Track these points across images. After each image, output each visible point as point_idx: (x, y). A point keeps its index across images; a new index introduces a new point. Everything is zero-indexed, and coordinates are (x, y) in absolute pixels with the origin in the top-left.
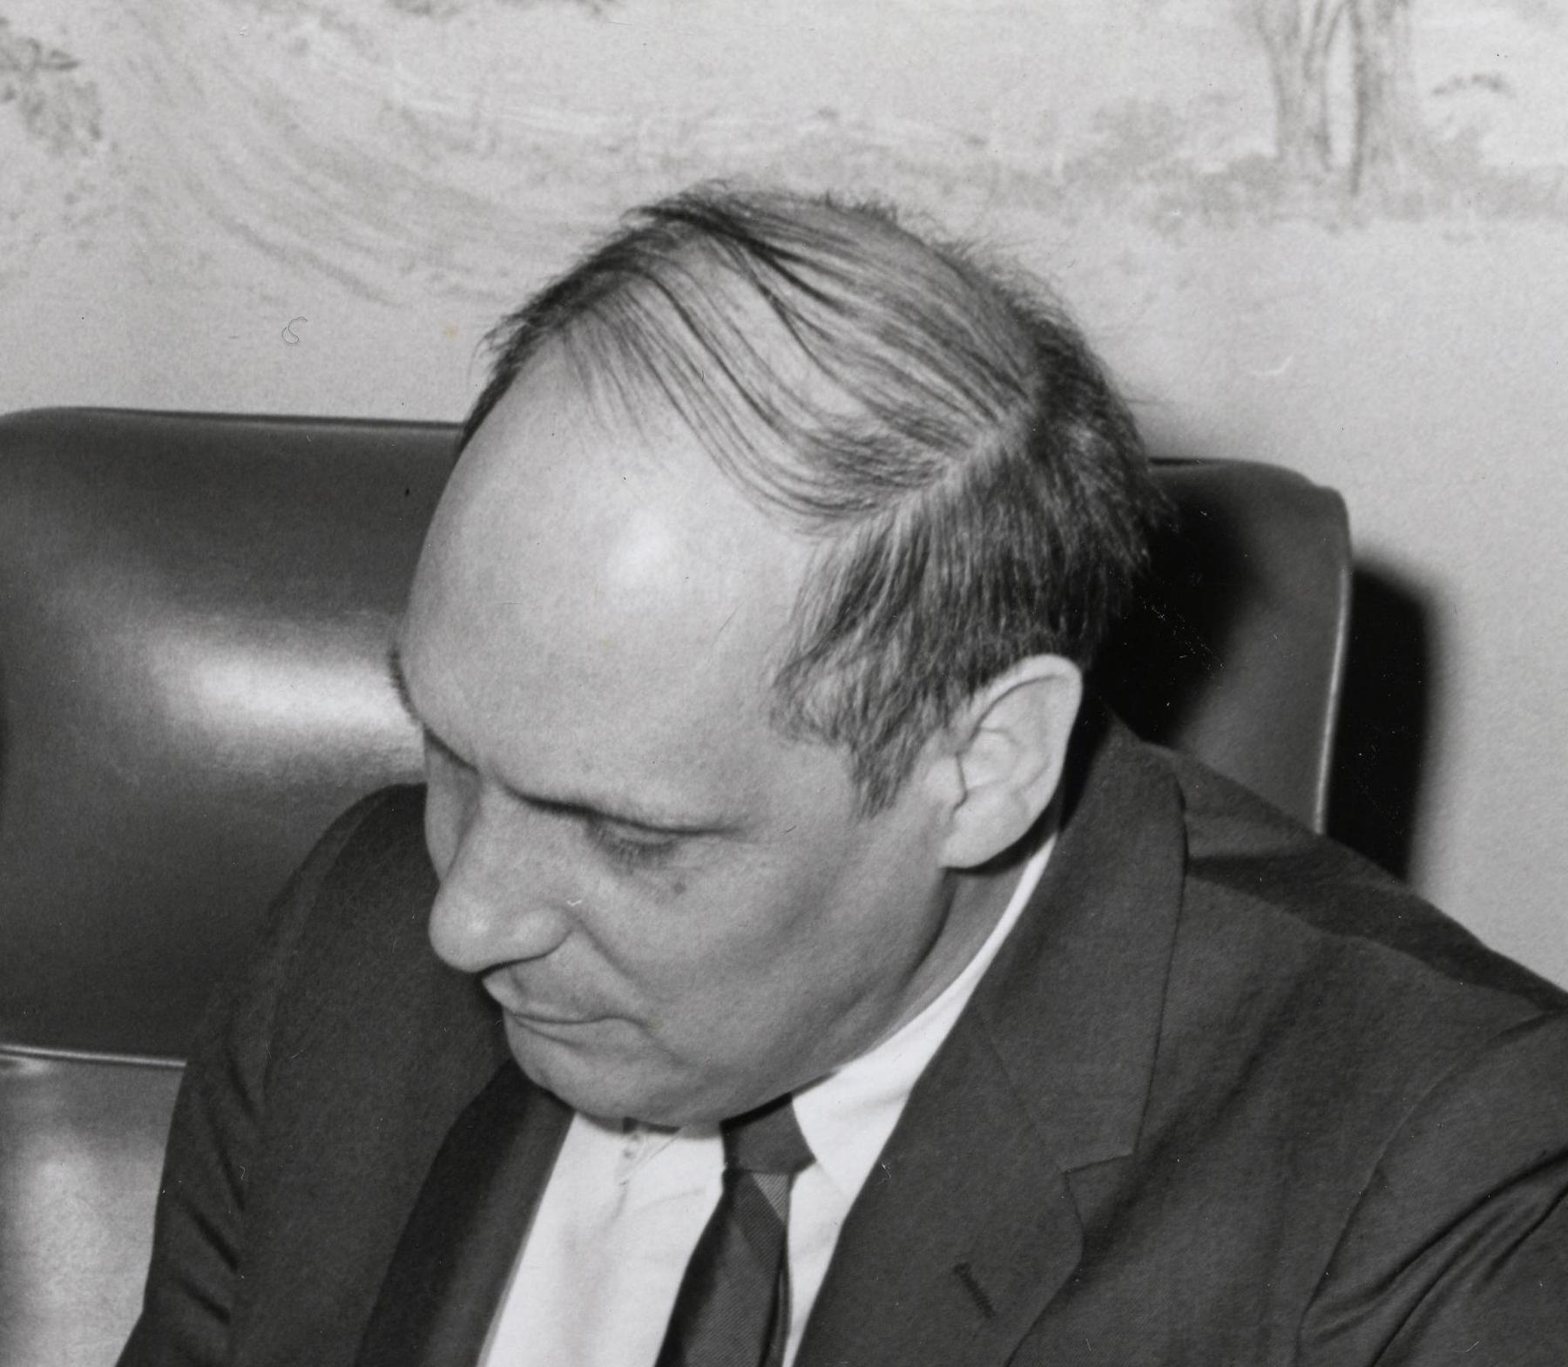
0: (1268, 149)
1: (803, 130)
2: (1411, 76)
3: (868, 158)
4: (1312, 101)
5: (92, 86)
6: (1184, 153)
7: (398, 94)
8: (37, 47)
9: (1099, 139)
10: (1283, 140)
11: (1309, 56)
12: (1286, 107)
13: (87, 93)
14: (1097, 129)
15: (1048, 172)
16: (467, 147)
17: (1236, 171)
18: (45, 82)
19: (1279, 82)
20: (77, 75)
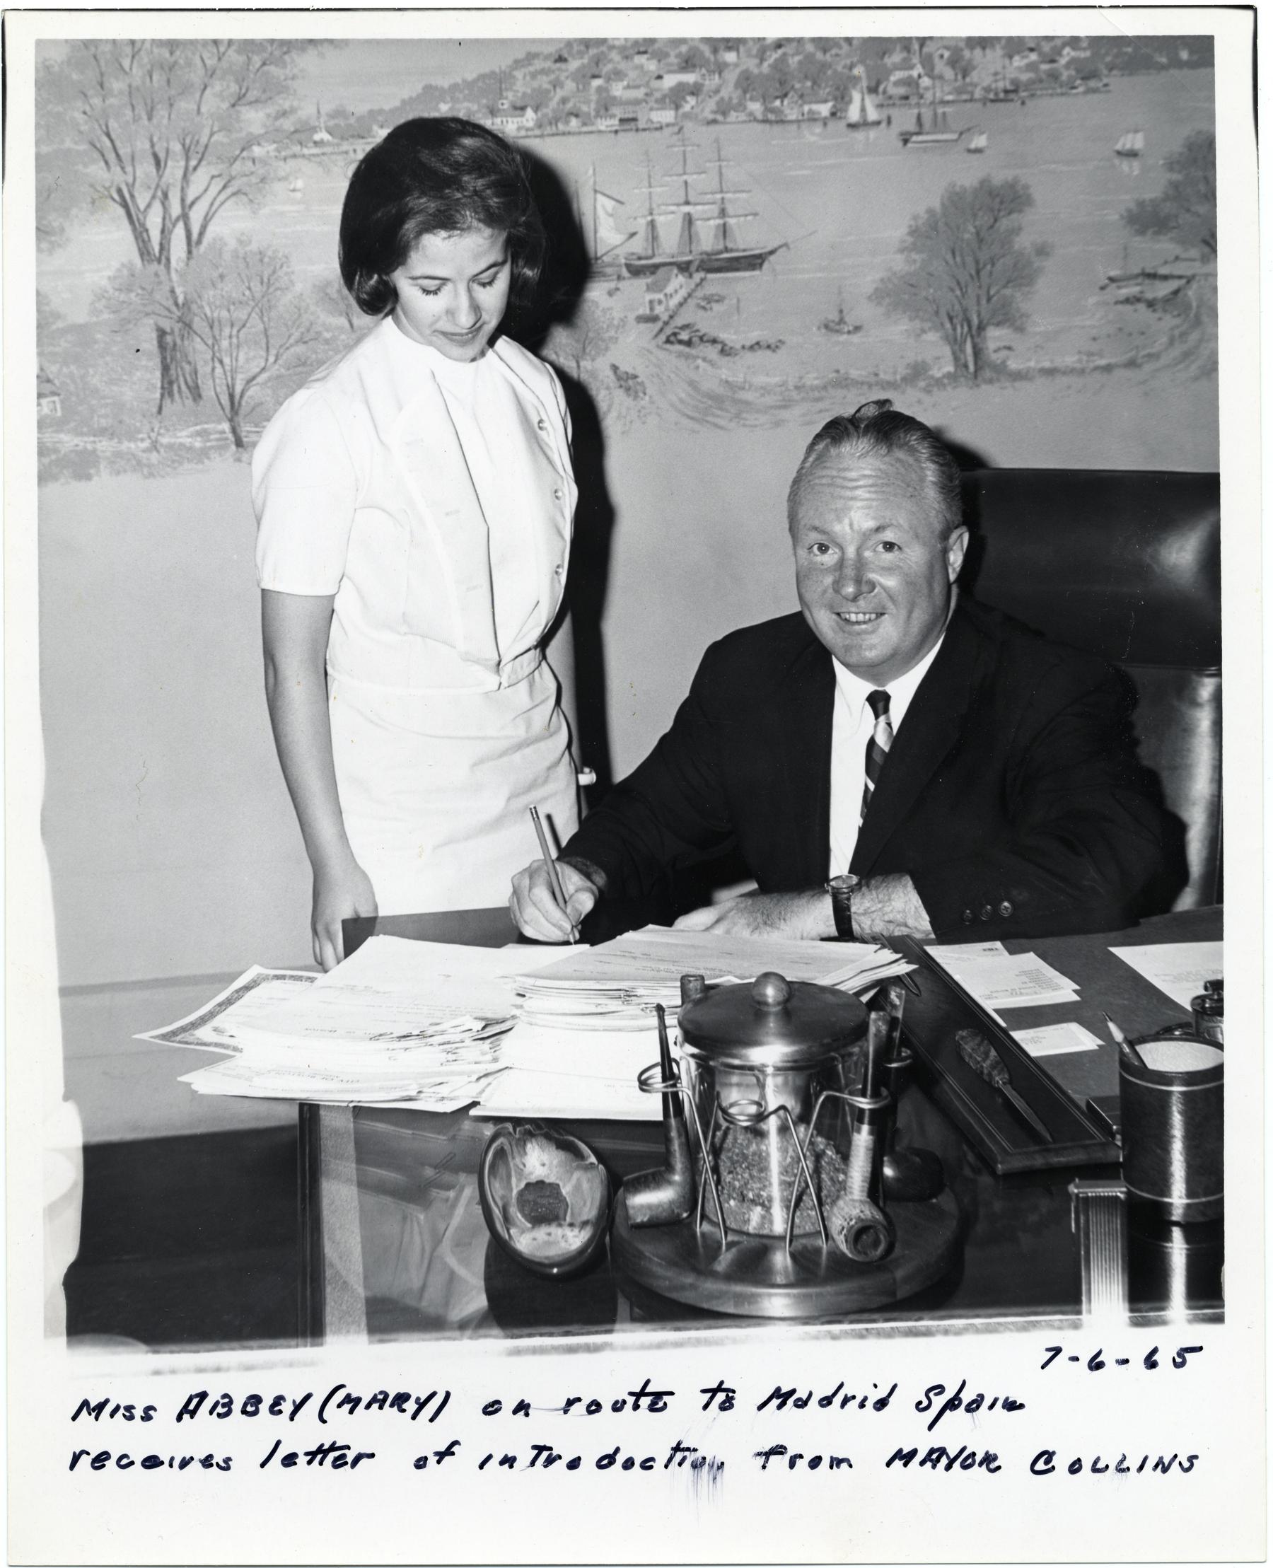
0: (950, 368)
2: (987, 348)
3: (849, 381)
4: (962, 356)
5: (643, 382)
6: (931, 373)
7: (724, 377)
8: (627, 373)
9: (909, 371)
10: (956, 366)
12: (956, 359)
13: (642, 384)
15: (896, 381)
16: (743, 388)
17: (944, 376)
18: (630, 382)
19: (954, 353)
20: (639, 380)
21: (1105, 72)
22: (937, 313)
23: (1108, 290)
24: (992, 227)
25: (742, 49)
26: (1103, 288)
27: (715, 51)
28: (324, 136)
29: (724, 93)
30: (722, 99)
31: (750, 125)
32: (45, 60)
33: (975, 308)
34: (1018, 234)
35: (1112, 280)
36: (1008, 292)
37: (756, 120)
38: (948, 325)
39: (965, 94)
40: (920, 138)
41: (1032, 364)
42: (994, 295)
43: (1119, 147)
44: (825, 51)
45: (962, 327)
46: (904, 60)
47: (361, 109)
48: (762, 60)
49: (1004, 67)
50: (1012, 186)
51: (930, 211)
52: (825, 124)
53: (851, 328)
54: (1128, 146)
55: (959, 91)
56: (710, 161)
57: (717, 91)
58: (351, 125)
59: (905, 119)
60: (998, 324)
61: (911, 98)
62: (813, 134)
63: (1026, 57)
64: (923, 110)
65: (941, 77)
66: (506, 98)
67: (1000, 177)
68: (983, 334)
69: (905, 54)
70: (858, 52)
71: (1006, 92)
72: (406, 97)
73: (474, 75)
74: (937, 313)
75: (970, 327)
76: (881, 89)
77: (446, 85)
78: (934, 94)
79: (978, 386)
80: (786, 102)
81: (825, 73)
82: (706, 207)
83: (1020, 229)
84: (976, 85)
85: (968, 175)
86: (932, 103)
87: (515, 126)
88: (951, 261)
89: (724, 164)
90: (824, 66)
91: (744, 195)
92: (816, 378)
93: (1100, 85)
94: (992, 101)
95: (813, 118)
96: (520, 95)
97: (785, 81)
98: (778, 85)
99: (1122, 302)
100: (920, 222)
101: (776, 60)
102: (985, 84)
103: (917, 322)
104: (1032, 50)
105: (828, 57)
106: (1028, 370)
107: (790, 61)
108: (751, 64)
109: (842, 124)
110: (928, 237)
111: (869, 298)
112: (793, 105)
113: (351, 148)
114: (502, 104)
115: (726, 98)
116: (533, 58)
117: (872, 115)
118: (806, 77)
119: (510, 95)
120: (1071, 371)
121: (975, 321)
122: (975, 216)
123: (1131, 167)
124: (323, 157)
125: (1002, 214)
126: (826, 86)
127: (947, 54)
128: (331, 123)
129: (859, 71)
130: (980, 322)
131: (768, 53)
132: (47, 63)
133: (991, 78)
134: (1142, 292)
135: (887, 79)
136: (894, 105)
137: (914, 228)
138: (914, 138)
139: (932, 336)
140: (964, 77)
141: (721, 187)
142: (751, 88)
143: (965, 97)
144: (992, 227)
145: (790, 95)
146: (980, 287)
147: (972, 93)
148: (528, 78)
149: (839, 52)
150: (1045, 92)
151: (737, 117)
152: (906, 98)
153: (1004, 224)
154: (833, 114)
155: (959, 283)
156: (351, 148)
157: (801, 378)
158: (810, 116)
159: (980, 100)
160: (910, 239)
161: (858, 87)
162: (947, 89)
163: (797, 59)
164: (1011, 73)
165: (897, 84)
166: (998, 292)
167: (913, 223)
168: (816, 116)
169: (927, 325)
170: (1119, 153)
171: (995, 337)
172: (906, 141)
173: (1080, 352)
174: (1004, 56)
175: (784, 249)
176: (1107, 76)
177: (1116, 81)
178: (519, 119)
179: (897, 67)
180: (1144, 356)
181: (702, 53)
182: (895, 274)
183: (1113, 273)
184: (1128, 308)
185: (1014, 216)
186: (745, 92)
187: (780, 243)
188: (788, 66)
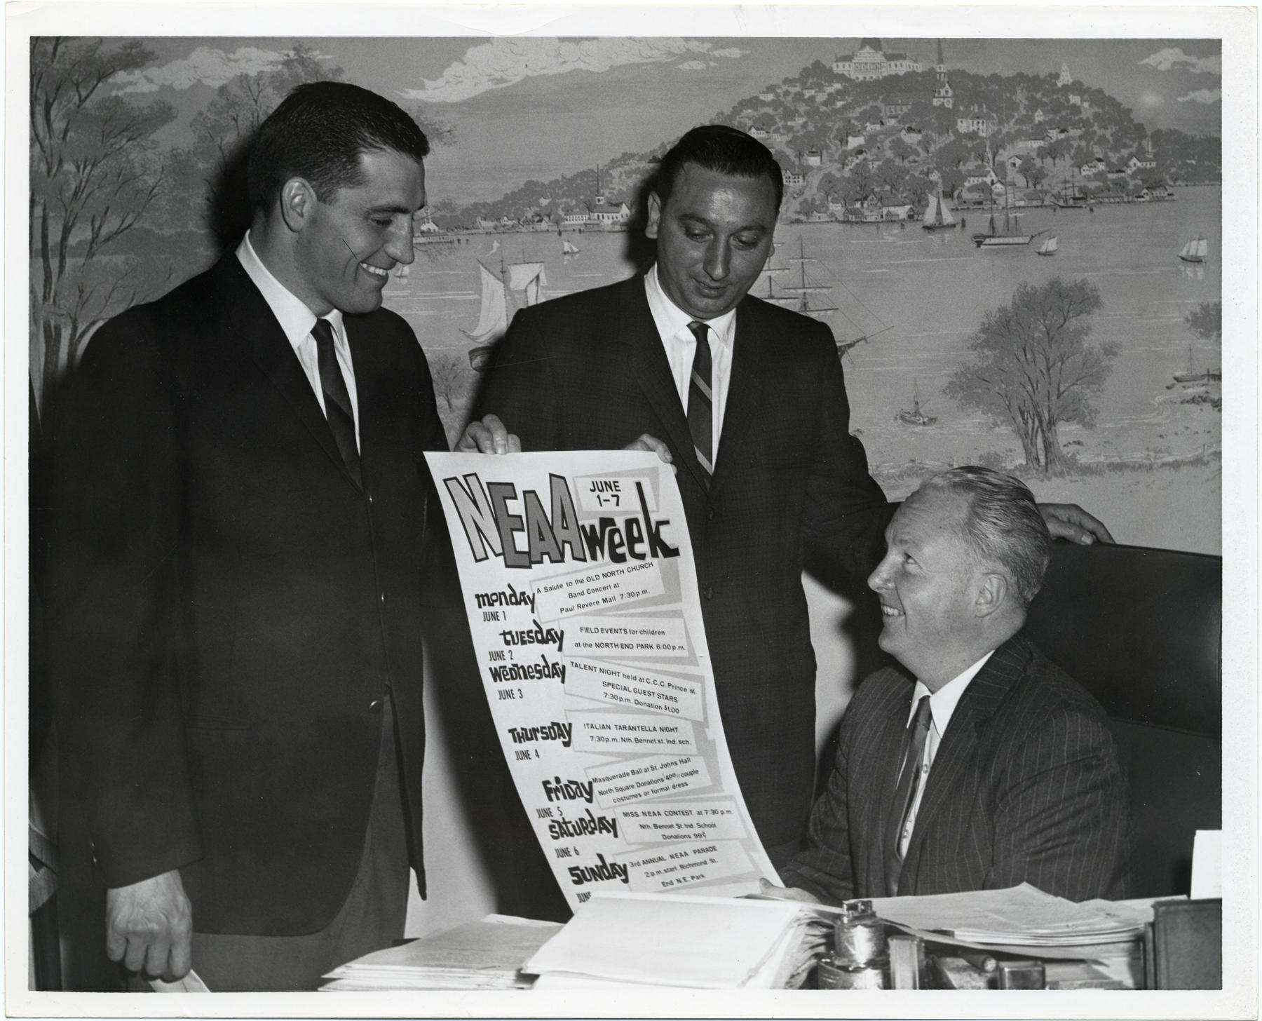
0: (1024, 463)
1: (906, 465)
3: (923, 471)
4: (1034, 450)
6: (1003, 465)
10: (1027, 460)
11: (1031, 440)
12: (1028, 452)
14: (981, 460)
17: (1016, 467)
19: (1025, 446)
21: (1172, 183)
22: (1009, 407)
23: (1174, 390)
24: (1062, 326)
25: (824, 152)
26: (1168, 388)
27: (800, 155)
28: (433, 227)
29: (807, 195)
30: (806, 200)
31: (833, 224)
32: (174, 149)
33: (1046, 404)
34: (1086, 334)
35: (1176, 379)
36: (1077, 388)
37: (839, 222)
38: (1020, 419)
39: (1037, 199)
40: (993, 241)
41: (1102, 459)
42: (1063, 393)
43: (1183, 253)
44: (903, 159)
45: (1033, 422)
46: (978, 167)
47: (466, 201)
48: (843, 168)
49: (1073, 176)
50: (1081, 287)
51: (1003, 310)
52: (903, 226)
53: (926, 420)
54: (1191, 254)
55: (1030, 198)
56: (793, 258)
57: (801, 193)
58: (457, 216)
59: (979, 221)
60: (1068, 421)
61: (984, 203)
62: (891, 235)
63: (1095, 167)
64: (995, 215)
65: (1013, 184)
66: (603, 195)
67: (1069, 278)
68: (1053, 428)
69: (980, 162)
70: (935, 159)
71: (1075, 199)
72: (509, 192)
73: (575, 172)
74: (1009, 407)
75: (1041, 422)
76: (956, 194)
77: (546, 183)
78: (1007, 203)
79: (1049, 479)
80: (865, 205)
81: (903, 179)
82: (789, 301)
83: (1089, 328)
84: (1046, 192)
85: (1038, 276)
86: (1003, 208)
87: (610, 221)
88: (1023, 359)
89: (807, 260)
90: (904, 171)
91: (825, 291)
92: (893, 468)
93: (1166, 194)
94: (1062, 207)
95: (891, 220)
96: (615, 192)
97: (865, 185)
98: (859, 188)
99: (1188, 402)
100: (993, 320)
101: (857, 164)
102: (1055, 192)
103: (990, 415)
104: (1100, 160)
105: (906, 163)
106: (1099, 462)
107: (871, 167)
108: (833, 169)
109: (919, 226)
110: (1003, 336)
111: (944, 391)
112: (871, 208)
113: (455, 238)
114: (599, 200)
115: (810, 200)
116: (629, 159)
117: (948, 218)
118: (885, 181)
119: (607, 192)
120: (1141, 466)
121: (1047, 416)
122: (1045, 315)
123: (1195, 272)
124: (430, 247)
125: (1071, 314)
126: (905, 190)
127: (1018, 162)
128: (438, 215)
129: (935, 177)
130: (1051, 417)
131: (850, 159)
132: (175, 152)
133: (1062, 186)
134: (1207, 392)
135: (964, 186)
136: (968, 208)
137: (987, 326)
138: (987, 241)
139: (1003, 430)
140: (1035, 185)
141: (804, 284)
142: (832, 191)
143: (1035, 203)
144: (1062, 326)
145: (870, 198)
146: (1050, 384)
147: (1043, 202)
148: (624, 175)
149: (917, 159)
150: (1112, 200)
151: (819, 217)
152: (980, 203)
153: (1073, 324)
154: (910, 217)
155: (1030, 380)
156: (455, 238)
157: (878, 467)
158: (889, 218)
159: (1050, 206)
160: (982, 336)
161: (934, 193)
162: (1019, 195)
163: (876, 164)
164: (1080, 182)
165: (970, 190)
166: (1068, 387)
167: (986, 321)
168: (893, 219)
169: (999, 419)
170: (1183, 259)
171: (1066, 432)
172: (979, 244)
173: (1147, 449)
174: (1072, 166)
175: (862, 342)
176: (1170, 186)
177: (1181, 190)
178: (614, 215)
179: (971, 174)
180: (1208, 456)
181: (788, 156)
182: (969, 368)
183: (1178, 374)
184: (1193, 407)
185: (1084, 316)
186: (827, 194)
187: (860, 335)
188: (869, 171)
